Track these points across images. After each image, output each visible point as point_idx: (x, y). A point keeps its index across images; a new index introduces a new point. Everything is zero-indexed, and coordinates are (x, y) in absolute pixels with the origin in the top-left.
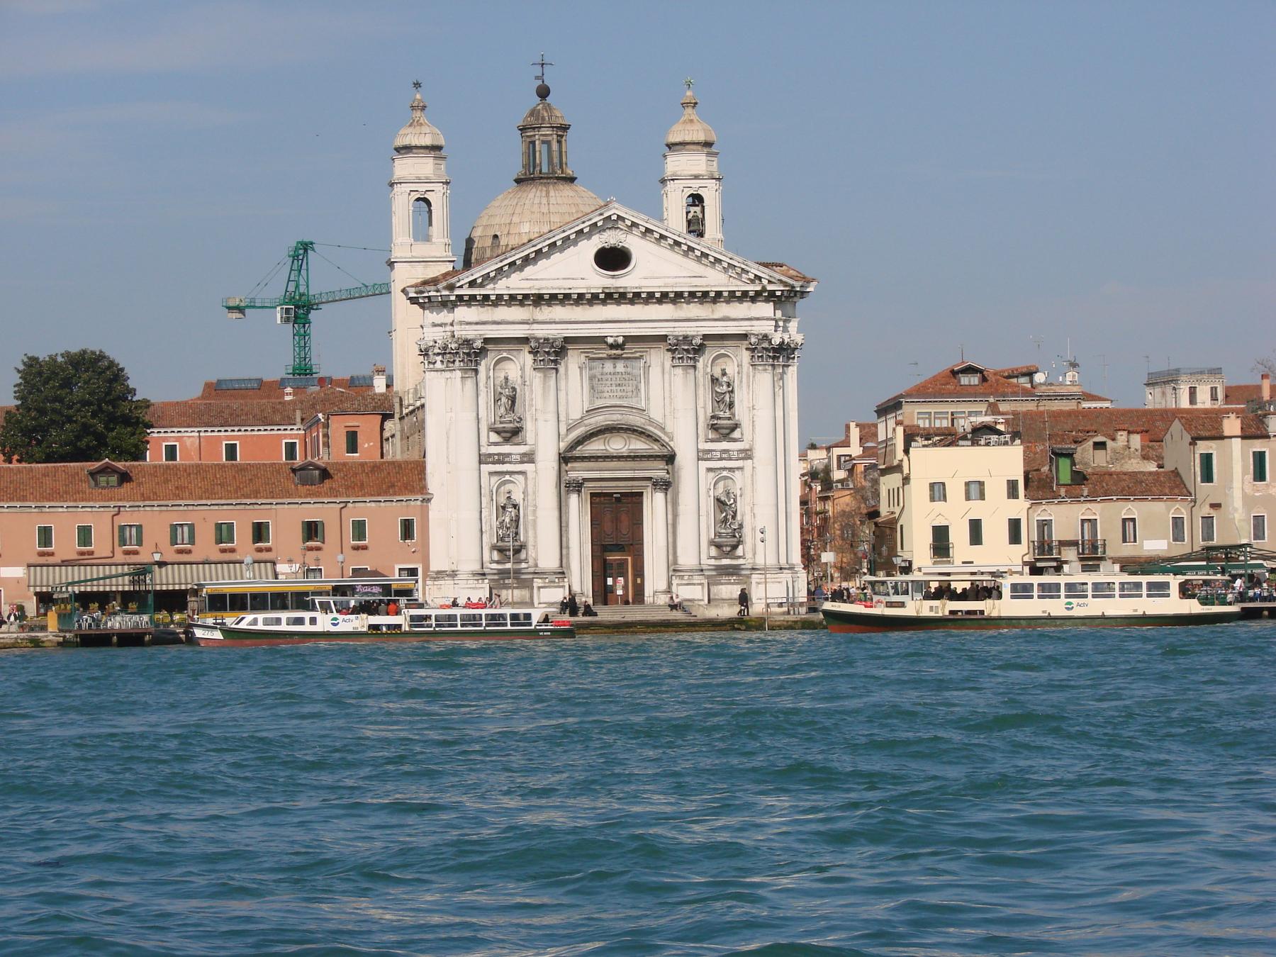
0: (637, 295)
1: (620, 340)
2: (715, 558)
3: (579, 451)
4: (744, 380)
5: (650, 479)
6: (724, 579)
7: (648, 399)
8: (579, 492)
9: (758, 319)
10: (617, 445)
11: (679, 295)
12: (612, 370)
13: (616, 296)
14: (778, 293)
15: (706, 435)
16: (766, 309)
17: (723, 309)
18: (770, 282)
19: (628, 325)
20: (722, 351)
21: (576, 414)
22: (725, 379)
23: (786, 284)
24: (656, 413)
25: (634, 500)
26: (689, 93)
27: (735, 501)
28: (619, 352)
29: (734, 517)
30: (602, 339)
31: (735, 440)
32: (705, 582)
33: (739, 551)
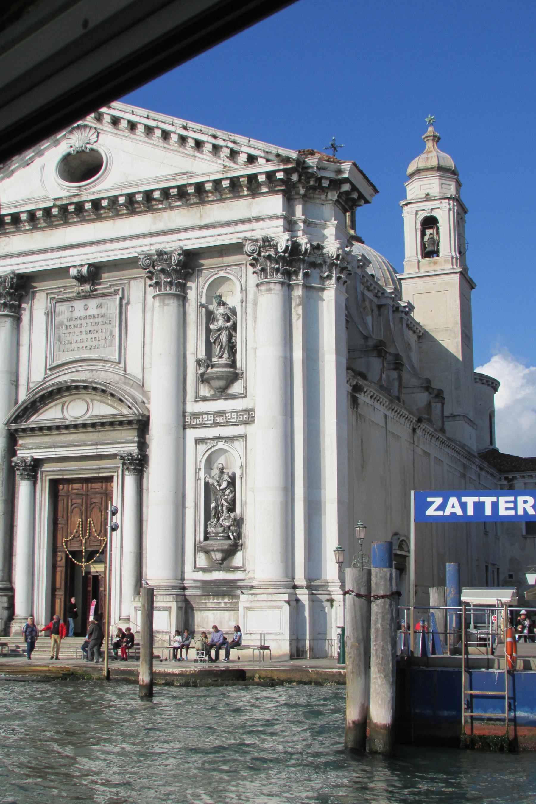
0: (96, 204)
1: (85, 270)
2: (203, 570)
3: (34, 421)
4: (249, 311)
5: (113, 456)
6: (211, 602)
7: (122, 348)
8: (34, 479)
9: (259, 219)
10: (76, 410)
11: (148, 195)
12: (82, 313)
13: (71, 208)
14: (280, 175)
15: (197, 392)
16: (274, 204)
17: (216, 212)
18: (268, 161)
19: (93, 249)
20: (222, 274)
21: (38, 376)
22: (221, 310)
23: (287, 160)
24: (133, 367)
25: (98, 488)
26: (430, 129)
27: (232, 483)
28: (87, 287)
29: (232, 508)
30: (62, 272)
31: (234, 397)
32: (173, 605)
33: (237, 560)
